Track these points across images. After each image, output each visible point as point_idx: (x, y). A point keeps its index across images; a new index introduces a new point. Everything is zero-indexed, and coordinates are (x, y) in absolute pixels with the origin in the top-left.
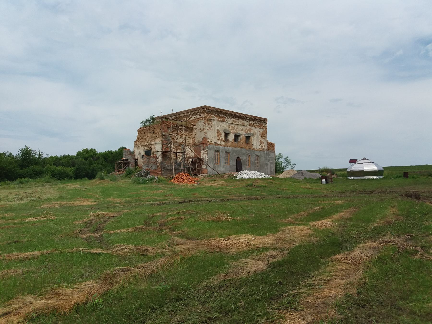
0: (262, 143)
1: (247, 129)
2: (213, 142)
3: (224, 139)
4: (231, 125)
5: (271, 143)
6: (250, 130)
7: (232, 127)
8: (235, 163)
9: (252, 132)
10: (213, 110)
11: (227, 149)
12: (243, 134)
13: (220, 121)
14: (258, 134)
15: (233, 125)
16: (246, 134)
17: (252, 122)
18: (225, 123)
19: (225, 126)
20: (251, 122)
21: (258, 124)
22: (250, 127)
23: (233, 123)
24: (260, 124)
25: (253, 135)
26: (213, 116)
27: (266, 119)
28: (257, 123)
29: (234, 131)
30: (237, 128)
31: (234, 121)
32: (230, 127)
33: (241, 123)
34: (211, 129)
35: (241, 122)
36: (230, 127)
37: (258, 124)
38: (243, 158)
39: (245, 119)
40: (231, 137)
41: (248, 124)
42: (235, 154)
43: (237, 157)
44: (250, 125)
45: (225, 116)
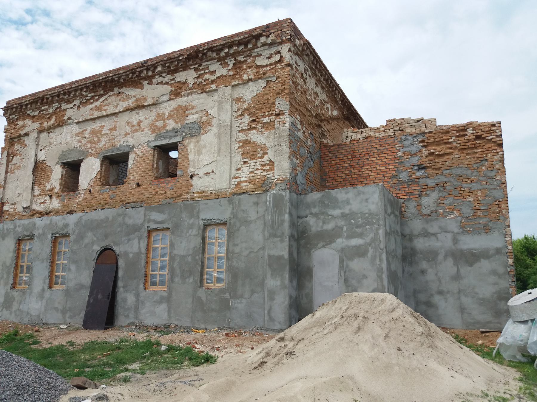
0: (251, 151)
1: (160, 117)
2: (20, 209)
4: (90, 127)
5: (462, 130)
6: (182, 112)
7: (93, 132)
8: (86, 277)
9: (192, 118)
10: (21, 105)
11: (60, 224)
13: (49, 130)
15: (97, 125)
16: (158, 137)
17: (189, 76)
18: (66, 129)
20: (181, 76)
22: (180, 101)
23: (96, 114)
24: (238, 65)
25: (197, 129)
28: (215, 66)
31: (98, 109)
32: (87, 134)
33: (130, 103)
36: (87, 134)
37: (221, 71)
38: (128, 248)
39: (150, 79)
41: (167, 89)
42: (89, 237)
43: (97, 248)
44: (176, 94)
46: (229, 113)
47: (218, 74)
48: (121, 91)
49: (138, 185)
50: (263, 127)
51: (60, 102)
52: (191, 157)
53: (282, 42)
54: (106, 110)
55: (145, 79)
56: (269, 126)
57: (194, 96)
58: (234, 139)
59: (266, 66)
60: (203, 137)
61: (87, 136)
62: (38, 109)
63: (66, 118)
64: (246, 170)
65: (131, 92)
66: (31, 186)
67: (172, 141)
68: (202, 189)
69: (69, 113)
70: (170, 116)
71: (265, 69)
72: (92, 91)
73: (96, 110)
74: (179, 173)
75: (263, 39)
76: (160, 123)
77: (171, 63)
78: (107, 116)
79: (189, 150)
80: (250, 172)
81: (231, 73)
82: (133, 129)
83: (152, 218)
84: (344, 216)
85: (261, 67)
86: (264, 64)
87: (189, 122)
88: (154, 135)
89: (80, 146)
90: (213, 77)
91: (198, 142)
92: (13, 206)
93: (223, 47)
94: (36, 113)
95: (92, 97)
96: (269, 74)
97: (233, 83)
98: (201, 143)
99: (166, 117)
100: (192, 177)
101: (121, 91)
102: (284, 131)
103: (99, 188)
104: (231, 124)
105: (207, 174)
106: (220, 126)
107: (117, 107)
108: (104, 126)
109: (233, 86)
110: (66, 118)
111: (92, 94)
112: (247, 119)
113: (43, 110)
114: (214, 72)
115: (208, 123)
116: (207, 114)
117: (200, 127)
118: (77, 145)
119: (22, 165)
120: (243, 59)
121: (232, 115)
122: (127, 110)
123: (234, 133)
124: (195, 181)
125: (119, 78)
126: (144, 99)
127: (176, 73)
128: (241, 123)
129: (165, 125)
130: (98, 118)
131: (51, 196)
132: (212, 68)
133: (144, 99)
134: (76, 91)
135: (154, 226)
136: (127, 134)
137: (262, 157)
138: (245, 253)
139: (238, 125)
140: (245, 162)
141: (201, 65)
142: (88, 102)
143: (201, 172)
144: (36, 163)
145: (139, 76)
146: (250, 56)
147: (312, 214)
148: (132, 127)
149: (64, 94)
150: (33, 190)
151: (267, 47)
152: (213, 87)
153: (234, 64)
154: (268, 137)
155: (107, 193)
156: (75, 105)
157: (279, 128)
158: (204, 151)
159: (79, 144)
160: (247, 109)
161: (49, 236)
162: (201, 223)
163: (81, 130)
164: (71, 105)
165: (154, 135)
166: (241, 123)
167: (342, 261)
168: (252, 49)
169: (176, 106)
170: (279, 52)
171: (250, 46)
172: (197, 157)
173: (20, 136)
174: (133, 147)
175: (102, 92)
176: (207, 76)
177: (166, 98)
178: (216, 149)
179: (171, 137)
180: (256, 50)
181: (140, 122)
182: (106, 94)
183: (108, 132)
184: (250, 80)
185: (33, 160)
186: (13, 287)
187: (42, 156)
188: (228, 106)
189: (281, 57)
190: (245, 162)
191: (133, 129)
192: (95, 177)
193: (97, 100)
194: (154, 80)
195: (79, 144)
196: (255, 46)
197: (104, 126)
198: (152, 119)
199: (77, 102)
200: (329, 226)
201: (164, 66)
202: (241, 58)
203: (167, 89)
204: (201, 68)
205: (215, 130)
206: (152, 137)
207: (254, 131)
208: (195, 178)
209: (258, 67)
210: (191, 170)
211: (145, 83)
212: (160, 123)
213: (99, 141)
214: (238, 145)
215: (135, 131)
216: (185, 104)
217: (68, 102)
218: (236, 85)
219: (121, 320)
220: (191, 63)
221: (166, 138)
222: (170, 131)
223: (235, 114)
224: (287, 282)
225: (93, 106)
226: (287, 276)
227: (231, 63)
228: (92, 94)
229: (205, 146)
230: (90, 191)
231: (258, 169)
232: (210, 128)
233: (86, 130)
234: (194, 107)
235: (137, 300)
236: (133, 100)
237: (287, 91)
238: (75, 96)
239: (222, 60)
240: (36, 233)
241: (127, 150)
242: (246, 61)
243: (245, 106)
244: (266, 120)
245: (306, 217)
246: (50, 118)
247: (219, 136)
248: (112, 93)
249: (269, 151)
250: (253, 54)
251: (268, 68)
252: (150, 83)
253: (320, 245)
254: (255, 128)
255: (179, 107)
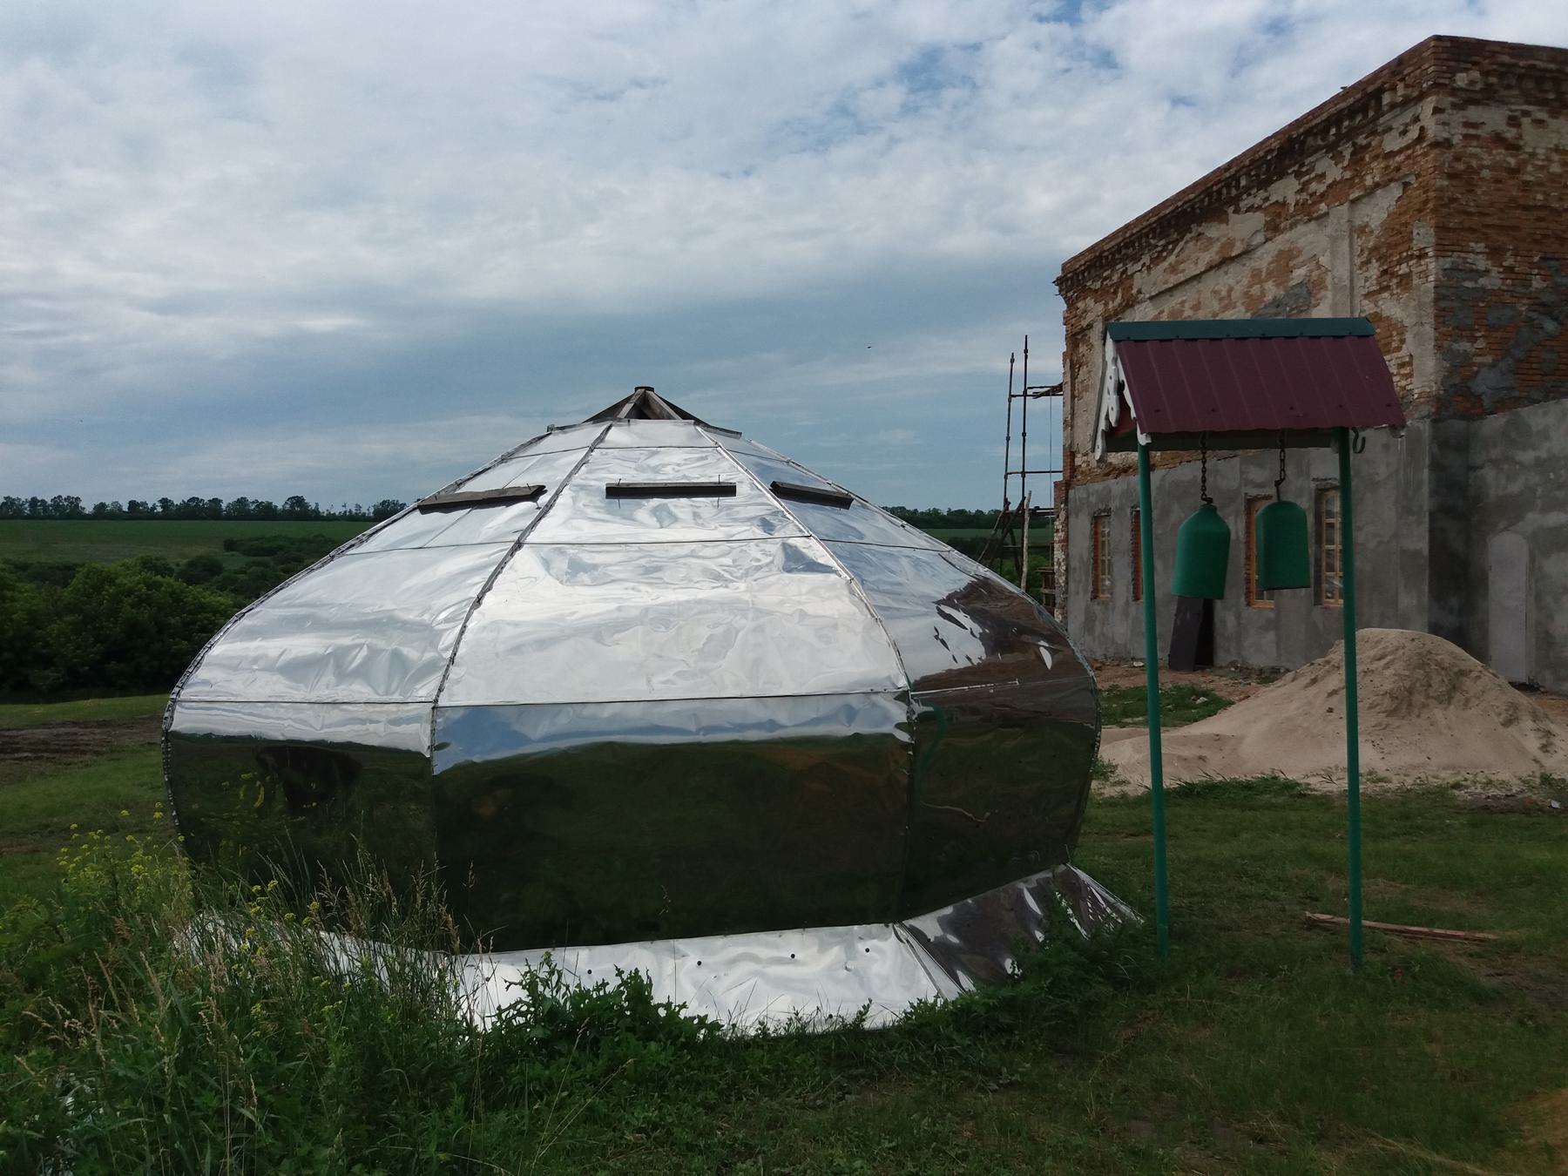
9: (1299, 274)
17: (1286, 190)
21: (1334, 173)
22: (1281, 242)
23: (1173, 280)
31: (1173, 269)
41: (1258, 219)
44: (1273, 229)
46: (1347, 261)
47: (1329, 181)
50: (1399, 285)
51: (1123, 260)
53: (1422, 96)
57: (1301, 228)
59: (1400, 151)
62: (1099, 276)
63: (1134, 291)
65: (1213, 231)
69: (1138, 281)
71: (1398, 159)
72: (1163, 235)
75: (1386, 99)
77: (1259, 168)
78: (1187, 281)
81: (1348, 175)
83: (1251, 477)
84: (1539, 464)
85: (1392, 154)
86: (1396, 148)
90: (1322, 188)
93: (1328, 123)
95: (1165, 247)
96: (1404, 170)
97: (1352, 197)
104: (1352, 281)
109: (1353, 202)
110: (1134, 291)
112: (1374, 269)
114: (1323, 176)
116: (1319, 266)
120: (1364, 142)
121: (1351, 261)
122: (1212, 267)
123: (1357, 300)
125: (1193, 207)
126: (1230, 243)
128: (1366, 280)
129: (1263, 294)
130: (1176, 287)
132: (1319, 170)
133: (1230, 243)
134: (1140, 238)
135: (1253, 492)
137: (1399, 349)
138: (1372, 545)
141: (1302, 165)
142: (1157, 260)
145: (1219, 199)
146: (1374, 133)
147: (1490, 461)
148: (1221, 300)
149: (1126, 247)
151: (1398, 111)
152: (1323, 207)
153: (1353, 154)
157: (1418, 287)
160: (1375, 249)
161: (1128, 511)
162: (1313, 485)
167: (1532, 560)
168: (1376, 118)
171: (1371, 114)
173: (1083, 330)
177: (1259, 238)
180: (1382, 120)
184: (1377, 186)
186: (1095, 597)
199: (1146, 259)
200: (1515, 488)
201: (1248, 174)
202: (1361, 140)
203: (1258, 219)
207: (1386, 295)
217: (1136, 259)
218: (1358, 199)
219: (1222, 658)
223: (1358, 261)
224: (1426, 599)
226: (1426, 588)
235: (1239, 624)
236: (1216, 247)
237: (1430, 205)
238: (1141, 248)
239: (1332, 149)
240: (1113, 505)
245: (1482, 467)
246: (1115, 293)
249: (1409, 336)
250: (1380, 129)
252: (1237, 211)
253: (1501, 526)
254: (1387, 288)
255: (1281, 252)
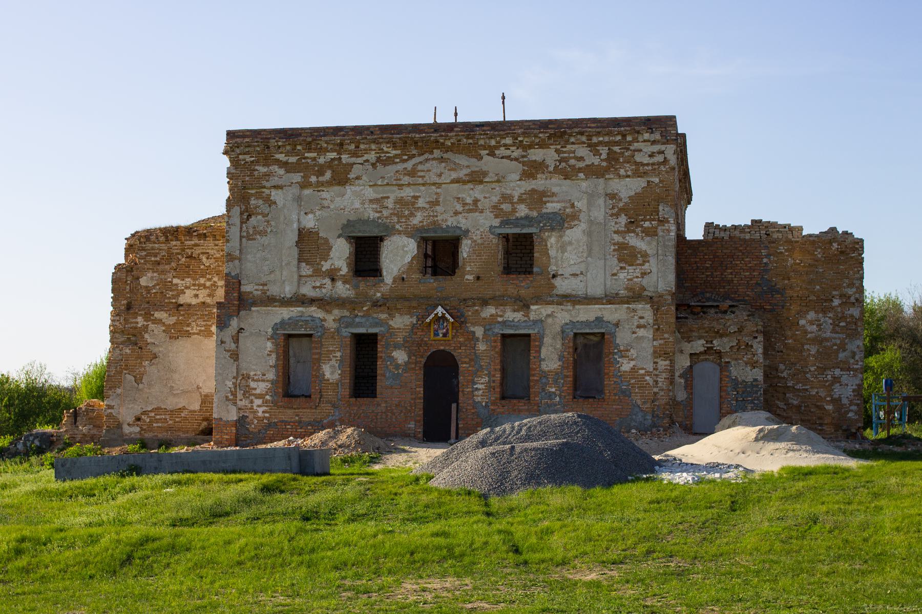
0: (628, 256)
1: (506, 198)
3: (345, 270)
6: (537, 198)
7: (400, 201)
9: (552, 207)
12: (479, 231)
14: (599, 212)
16: (504, 223)
17: (549, 155)
19: (356, 200)
24: (612, 158)
25: (560, 222)
26: (275, 168)
27: (675, 117)
29: (416, 221)
30: (436, 203)
32: (390, 203)
33: (462, 174)
34: (263, 233)
35: (456, 167)
36: (390, 203)
40: (399, 255)
45: (345, 158)
47: (588, 162)
48: (445, 156)
49: (478, 278)
52: (552, 253)
54: (423, 177)
55: (484, 147)
56: (651, 233)
58: (608, 240)
59: (648, 165)
60: (568, 232)
61: (391, 206)
63: (351, 176)
64: (622, 275)
66: (295, 262)
67: (525, 231)
68: (569, 291)
70: (521, 200)
73: (405, 174)
74: (535, 270)
76: (506, 207)
79: (549, 246)
80: (628, 280)
81: (604, 164)
82: (467, 208)
85: (643, 165)
86: (645, 162)
87: (548, 211)
88: (498, 220)
89: (379, 218)
90: (581, 164)
91: (561, 237)
92: (261, 287)
94: (293, 159)
95: (396, 156)
98: (566, 239)
99: (515, 200)
100: (554, 276)
101: (445, 156)
102: (669, 240)
103: (416, 276)
105: (575, 275)
106: (591, 222)
107: (440, 175)
108: (419, 197)
111: (399, 152)
112: (623, 220)
113: (305, 158)
114: (581, 159)
115: (575, 217)
116: (573, 206)
117: (564, 221)
118: (373, 215)
119: (269, 230)
124: (557, 282)
127: (530, 148)
128: (616, 223)
129: (514, 210)
131: (333, 280)
136: (456, 213)
139: (613, 224)
140: (621, 268)
142: (389, 161)
143: (567, 271)
144: (301, 232)
146: (628, 149)
148: (465, 204)
150: (299, 268)
154: (649, 243)
155: (432, 283)
156: (367, 161)
157: (663, 237)
158: (569, 248)
159: (377, 215)
163: (379, 196)
164: (360, 160)
165: (498, 220)
166: (616, 223)
168: (630, 143)
169: (529, 189)
170: (663, 152)
172: (560, 255)
174: (467, 231)
175: (414, 152)
176: (572, 162)
178: (585, 247)
179: (523, 226)
180: (635, 144)
181: (476, 201)
182: (420, 155)
183: (427, 206)
185: (295, 226)
187: (309, 222)
188: (601, 201)
189: (665, 158)
190: (621, 268)
191: (467, 208)
192: (411, 263)
193: (406, 160)
194: (497, 152)
195: (377, 215)
196: (636, 140)
197: (419, 197)
198: (495, 199)
204: (564, 149)
205: (583, 226)
206: (496, 222)
208: (559, 278)
209: (636, 163)
210: (553, 268)
211: (484, 152)
212: (506, 207)
213: (412, 215)
214: (612, 247)
215: (470, 211)
216: (541, 189)
220: (551, 141)
221: (516, 226)
222: (521, 218)
223: (610, 212)
225: (400, 167)
227: (604, 151)
228: (399, 152)
229: (570, 243)
230: (403, 279)
231: (637, 277)
232: (576, 222)
233: (388, 197)
234: (553, 195)
241: (458, 233)
242: (623, 153)
243: (621, 205)
244: (647, 224)
247: (589, 234)
248: (431, 156)
251: (650, 168)
252: (492, 154)
254: (634, 231)
255: (533, 191)
